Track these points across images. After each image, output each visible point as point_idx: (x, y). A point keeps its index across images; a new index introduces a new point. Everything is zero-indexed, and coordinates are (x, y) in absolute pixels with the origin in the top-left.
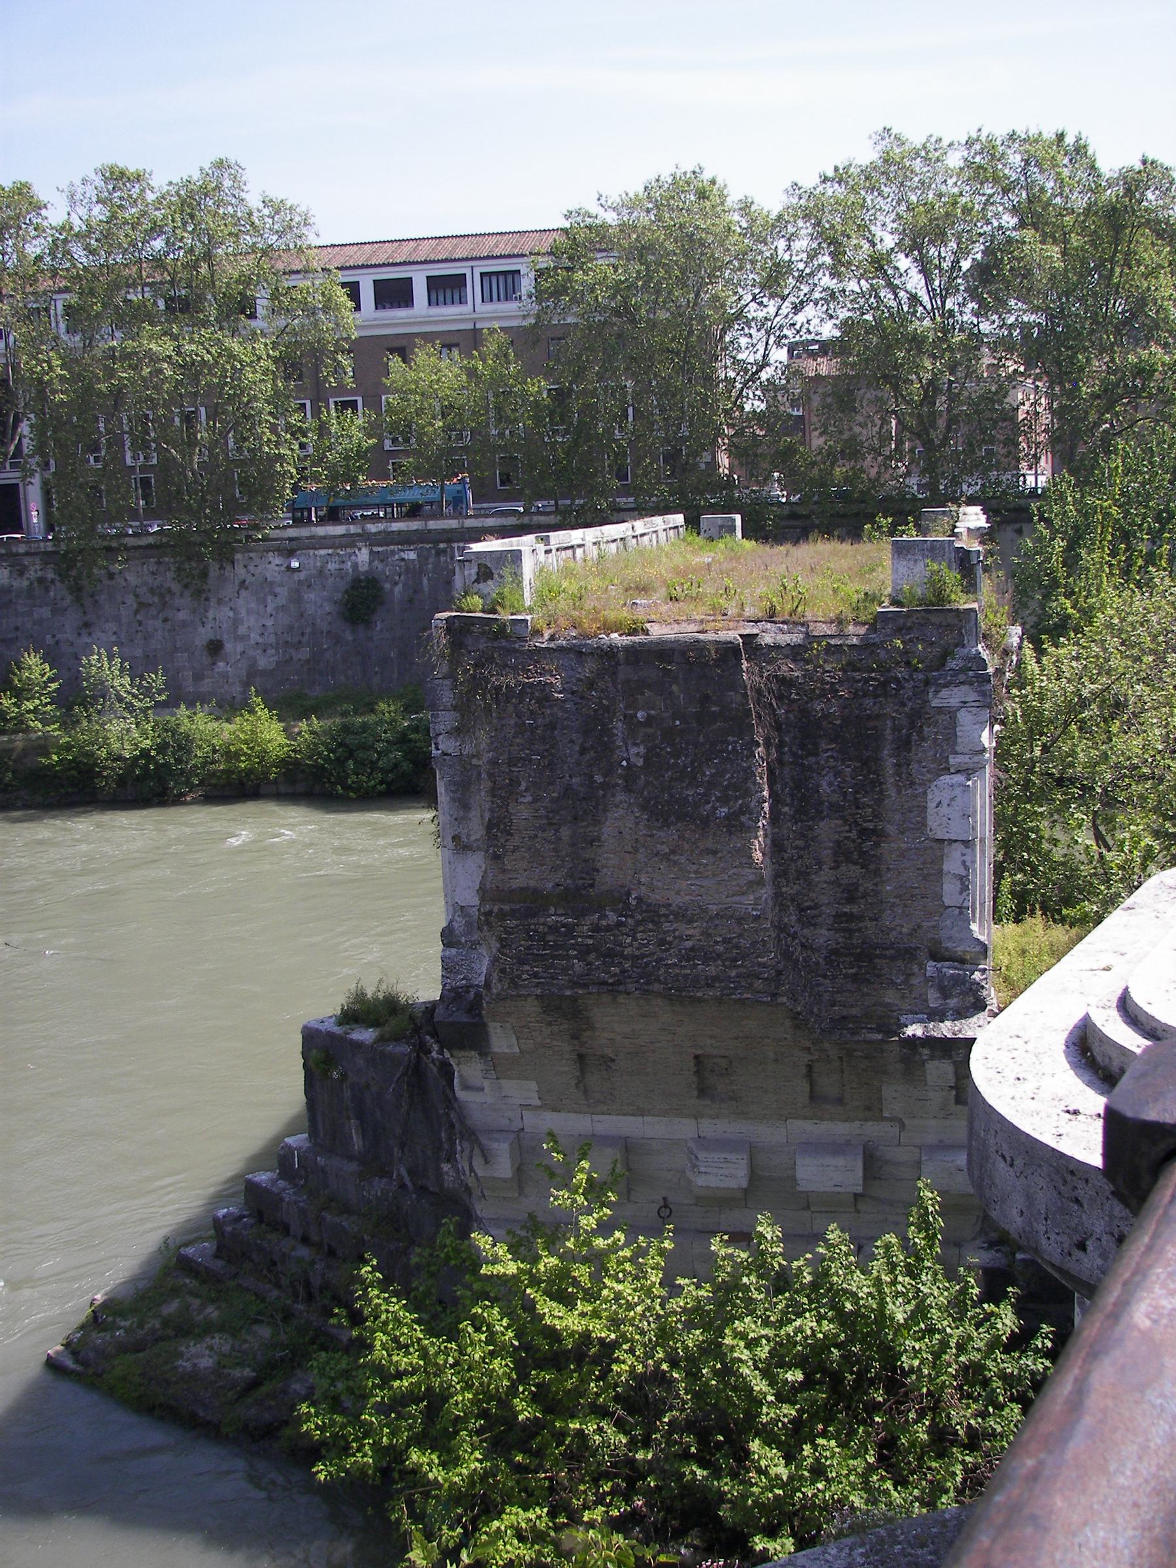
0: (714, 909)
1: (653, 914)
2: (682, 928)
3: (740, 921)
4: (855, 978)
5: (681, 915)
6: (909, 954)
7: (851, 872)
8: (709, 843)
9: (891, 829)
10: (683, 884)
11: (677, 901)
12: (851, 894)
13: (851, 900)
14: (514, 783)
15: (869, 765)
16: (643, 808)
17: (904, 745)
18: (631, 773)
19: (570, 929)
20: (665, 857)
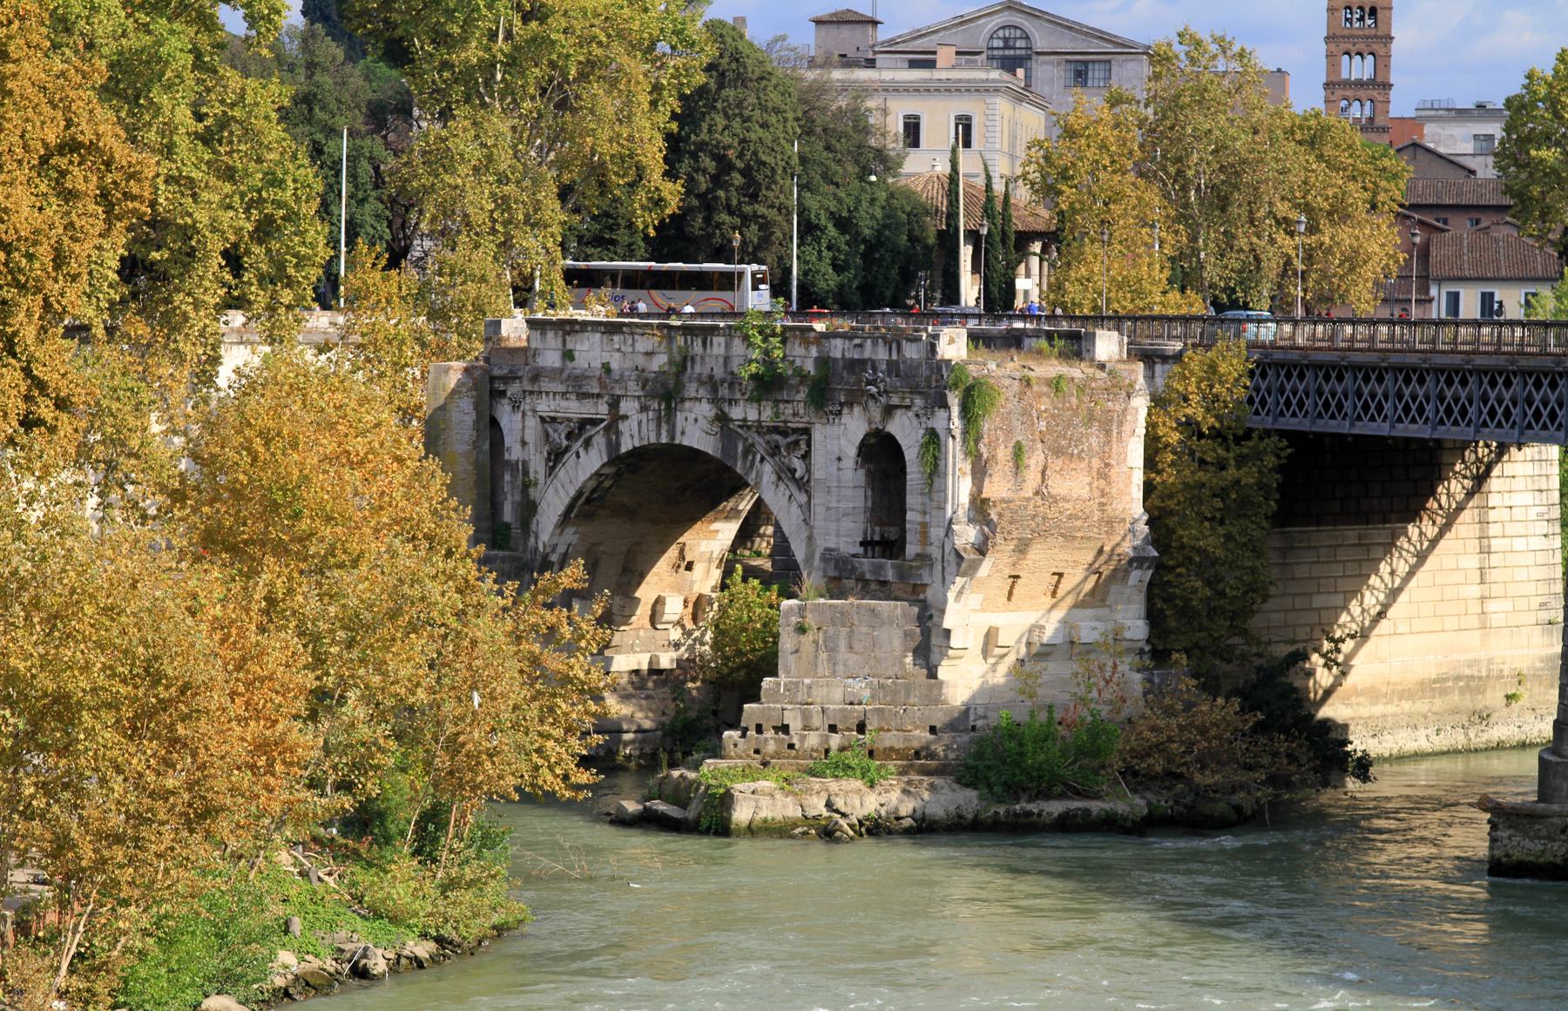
5: (1065, 499)
8: (1073, 466)
9: (1113, 462)
11: (1063, 493)
12: (1103, 494)
13: (1103, 496)
14: (997, 439)
15: (1108, 432)
17: (1120, 424)
19: (1025, 508)
20: (1058, 472)
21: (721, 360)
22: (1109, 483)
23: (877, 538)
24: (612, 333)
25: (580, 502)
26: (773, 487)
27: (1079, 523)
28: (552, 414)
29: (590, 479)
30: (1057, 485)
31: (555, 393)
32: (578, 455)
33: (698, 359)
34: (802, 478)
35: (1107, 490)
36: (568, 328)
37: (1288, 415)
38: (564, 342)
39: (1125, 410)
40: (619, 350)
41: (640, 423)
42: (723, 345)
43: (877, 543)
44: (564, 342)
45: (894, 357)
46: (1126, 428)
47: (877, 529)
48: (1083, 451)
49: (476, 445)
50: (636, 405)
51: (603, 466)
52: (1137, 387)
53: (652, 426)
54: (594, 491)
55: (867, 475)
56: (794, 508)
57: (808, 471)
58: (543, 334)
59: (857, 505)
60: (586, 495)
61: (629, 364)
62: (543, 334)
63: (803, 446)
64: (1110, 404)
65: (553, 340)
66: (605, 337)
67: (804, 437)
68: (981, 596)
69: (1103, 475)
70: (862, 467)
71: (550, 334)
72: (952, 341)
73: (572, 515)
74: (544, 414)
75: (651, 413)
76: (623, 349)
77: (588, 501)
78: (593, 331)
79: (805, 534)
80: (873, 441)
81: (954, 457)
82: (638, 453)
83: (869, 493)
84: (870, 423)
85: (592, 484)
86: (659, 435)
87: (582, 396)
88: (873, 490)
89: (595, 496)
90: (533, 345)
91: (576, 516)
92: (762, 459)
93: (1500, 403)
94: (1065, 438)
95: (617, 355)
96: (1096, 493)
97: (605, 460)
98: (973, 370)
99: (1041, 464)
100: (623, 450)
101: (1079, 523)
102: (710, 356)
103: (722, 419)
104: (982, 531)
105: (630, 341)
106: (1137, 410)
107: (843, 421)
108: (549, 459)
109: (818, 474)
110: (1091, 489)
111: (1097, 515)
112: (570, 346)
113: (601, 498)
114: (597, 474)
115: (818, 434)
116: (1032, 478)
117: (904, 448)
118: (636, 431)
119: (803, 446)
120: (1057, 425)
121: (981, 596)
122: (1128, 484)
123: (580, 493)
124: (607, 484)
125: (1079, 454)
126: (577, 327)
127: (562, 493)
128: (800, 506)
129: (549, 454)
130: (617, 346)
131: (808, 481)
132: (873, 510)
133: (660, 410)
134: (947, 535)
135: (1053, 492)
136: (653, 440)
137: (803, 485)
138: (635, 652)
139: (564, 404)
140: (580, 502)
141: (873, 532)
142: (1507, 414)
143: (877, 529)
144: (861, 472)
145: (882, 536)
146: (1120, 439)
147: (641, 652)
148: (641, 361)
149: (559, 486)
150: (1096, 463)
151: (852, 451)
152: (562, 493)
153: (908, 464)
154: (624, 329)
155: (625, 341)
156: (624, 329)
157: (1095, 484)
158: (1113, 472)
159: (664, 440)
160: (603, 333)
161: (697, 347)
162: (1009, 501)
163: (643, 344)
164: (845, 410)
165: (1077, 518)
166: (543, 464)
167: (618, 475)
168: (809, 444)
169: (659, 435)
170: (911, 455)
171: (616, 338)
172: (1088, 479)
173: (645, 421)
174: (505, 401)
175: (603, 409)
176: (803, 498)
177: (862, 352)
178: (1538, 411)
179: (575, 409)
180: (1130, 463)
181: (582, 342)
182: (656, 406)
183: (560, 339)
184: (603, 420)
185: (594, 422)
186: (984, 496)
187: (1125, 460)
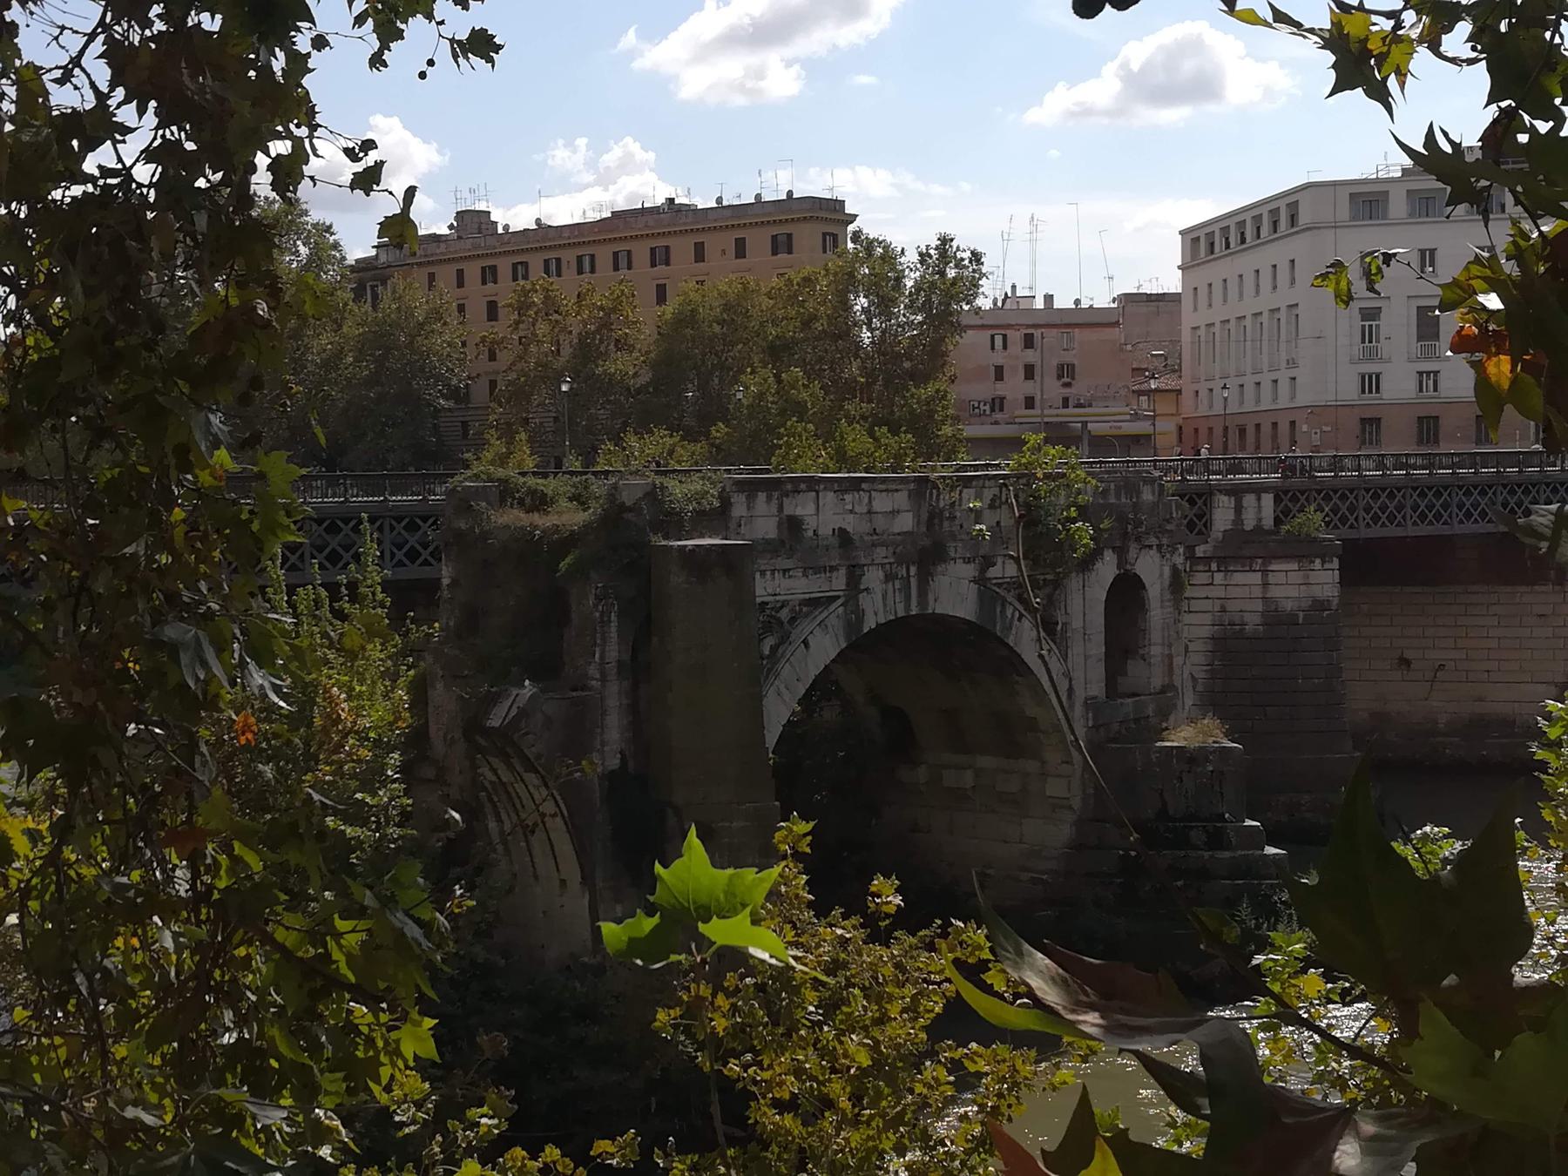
24: (846, 491)
32: (806, 643)
36: (789, 487)
40: (851, 511)
50: (881, 574)
75: (897, 584)
76: (857, 509)
86: (908, 607)
92: (1021, 616)
97: (844, 645)
103: (981, 580)
105: (866, 500)
118: (877, 609)
126: (803, 486)
127: (787, 695)
133: (909, 576)
136: (901, 613)
139: (786, 583)
149: (782, 687)
152: (787, 695)
154: (864, 486)
163: (882, 503)
169: (908, 607)
171: (848, 497)
175: (839, 581)
179: (800, 586)
184: (839, 597)
185: (814, 603)
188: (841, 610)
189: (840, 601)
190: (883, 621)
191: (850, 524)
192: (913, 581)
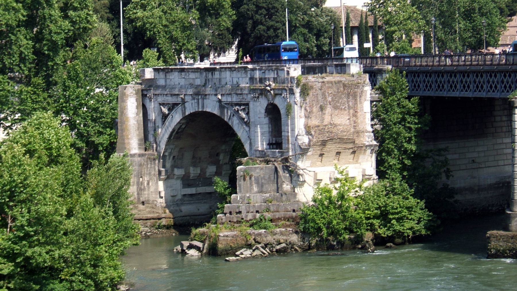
0: (343, 124)
1: (336, 125)
2: (341, 127)
3: (347, 125)
4: (357, 136)
5: (339, 125)
6: (363, 132)
7: (354, 118)
8: (342, 113)
9: (359, 111)
10: (339, 120)
11: (339, 123)
12: (355, 122)
13: (355, 123)
14: (313, 104)
15: (356, 100)
16: (333, 107)
17: (360, 97)
18: (330, 102)
19: (325, 129)
20: (337, 115)
21: (218, 80)
22: (357, 118)
23: (274, 142)
25: (174, 134)
26: (237, 125)
27: (345, 134)
28: (163, 102)
29: (177, 125)
30: (337, 120)
31: (163, 94)
33: (210, 80)
34: (247, 121)
35: (356, 121)
37: (427, 90)
38: (166, 76)
39: (362, 92)
40: (184, 78)
41: (192, 104)
42: (218, 74)
43: (274, 144)
44: (166, 76)
45: (276, 76)
46: (363, 98)
47: (274, 139)
48: (346, 107)
49: (137, 114)
51: (181, 120)
52: (366, 83)
53: (196, 105)
54: (179, 129)
55: (269, 120)
56: (245, 133)
57: (249, 118)
58: (159, 73)
59: (266, 130)
60: (176, 131)
61: (188, 83)
62: (159, 73)
63: (247, 110)
64: (356, 90)
65: (162, 75)
66: (179, 73)
67: (247, 107)
68: (310, 162)
69: (355, 115)
70: (267, 116)
71: (161, 73)
72: (295, 69)
73: (172, 138)
74: (160, 102)
75: (195, 100)
76: (185, 77)
77: (177, 133)
78: (175, 71)
79: (249, 142)
80: (270, 107)
81: (297, 112)
82: (191, 115)
83: (270, 126)
84: (268, 101)
85: (178, 126)
87: (172, 95)
88: (272, 124)
89: (180, 131)
90: (156, 78)
91: (173, 138)
93: (508, 83)
94: (339, 103)
95: (183, 80)
96: (352, 122)
98: (303, 81)
99: (330, 112)
100: (187, 114)
101: (345, 134)
102: (214, 78)
104: (309, 138)
105: (188, 75)
106: (366, 91)
107: (260, 100)
108: (162, 119)
109: (252, 120)
110: (350, 121)
111: (352, 130)
112: (168, 77)
113: (182, 132)
114: (179, 123)
115: (251, 106)
116: (327, 119)
117: (280, 109)
118: (190, 108)
119: (247, 110)
120: (336, 98)
121: (310, 162)
122: (365, 118)
123: (174, 130)
124: (183, 126)
125: (344, 108)
126: (170, 70)
128: (247, 132)
129: (163, 116)
130: (183, 77)
131: (249, 122)
132: (272, 132)
133: (198, 99)
134: (296, 140)
135: (335, 123)
136: (197, 110)
137: (247, 124)
138: (199, 187)
139: (167, 98)
140: (174, 134)
141: (272, 140)
142: (496, 87)
143: (274, 139)
144: (267, 119)
145: (276, 141)
146: (361, 103)
147: (202, 186)
148: (191, 81)
150: (352, 111)
151: (263, 111)
153: (282, 115)
155: (186, 75)
156: (185, 70)
157: (351, 119)
158: (359, 114)
159: (200, 110)
160: (179, 72)
161: (210, 76)
162: (318, 126)
164: (260, 97)
165: (345, 132)
166: (161, 120)
167: (187, 124)
168: (249, 110)
169: (198, 108)
170: (283, 111)
171: (183, 73)
172: (348, 118)
173: (194, 103)
174: (147, 98)
176: (247, 129)
177: (265, 75)
178: (439, 85)
180: (365, 111)
181: (172, 76)
182: (197, 97)
183: (164, 75)
184: (180, 104)
185: (177, 104)
186: (309, 125)
187: (363, 110)
188: (180, 107)
189: (180, 105)
190: (192, 112)
191: (183, 82)
192: (200, 101)
